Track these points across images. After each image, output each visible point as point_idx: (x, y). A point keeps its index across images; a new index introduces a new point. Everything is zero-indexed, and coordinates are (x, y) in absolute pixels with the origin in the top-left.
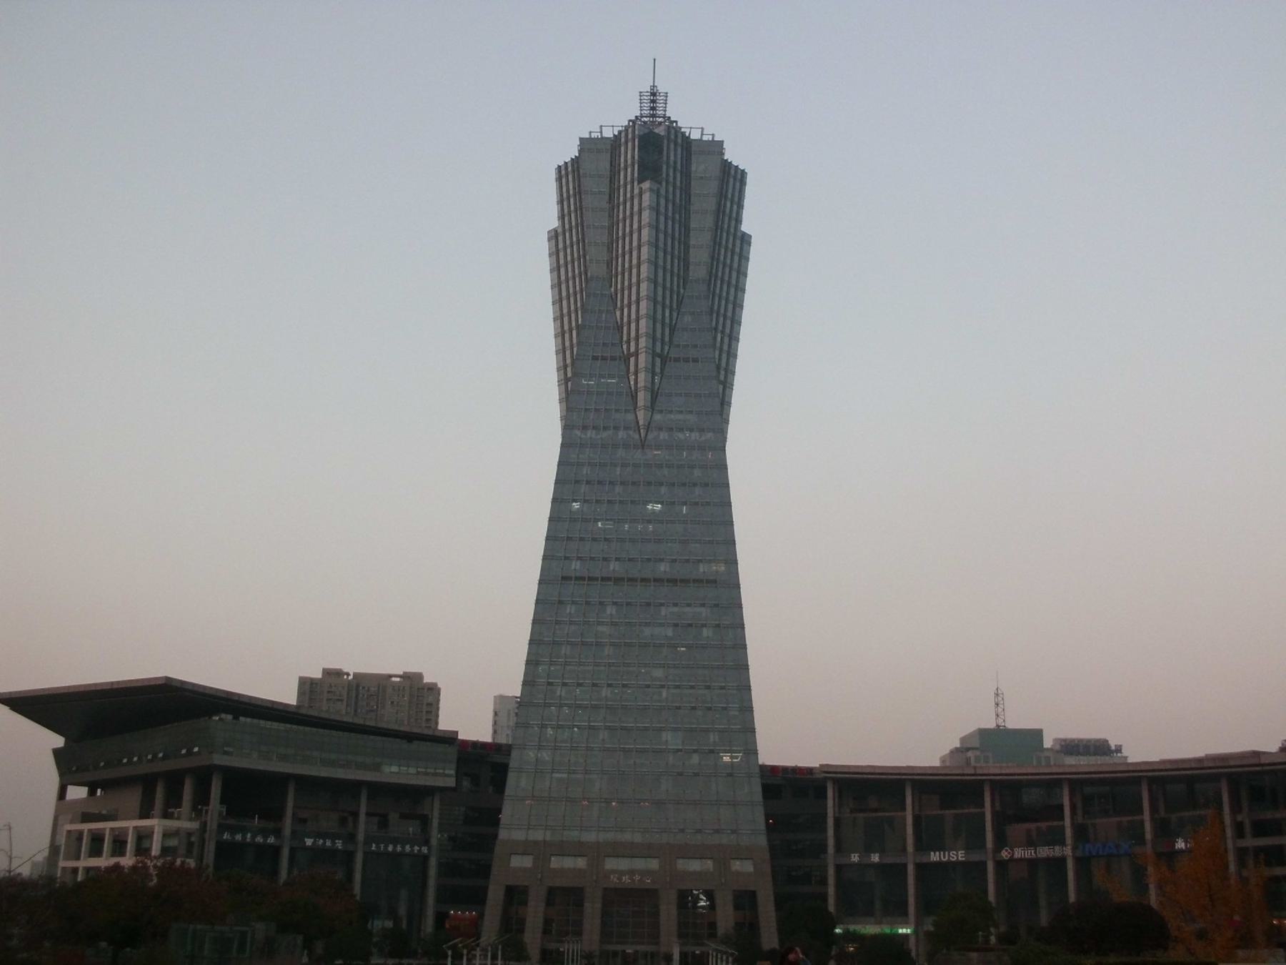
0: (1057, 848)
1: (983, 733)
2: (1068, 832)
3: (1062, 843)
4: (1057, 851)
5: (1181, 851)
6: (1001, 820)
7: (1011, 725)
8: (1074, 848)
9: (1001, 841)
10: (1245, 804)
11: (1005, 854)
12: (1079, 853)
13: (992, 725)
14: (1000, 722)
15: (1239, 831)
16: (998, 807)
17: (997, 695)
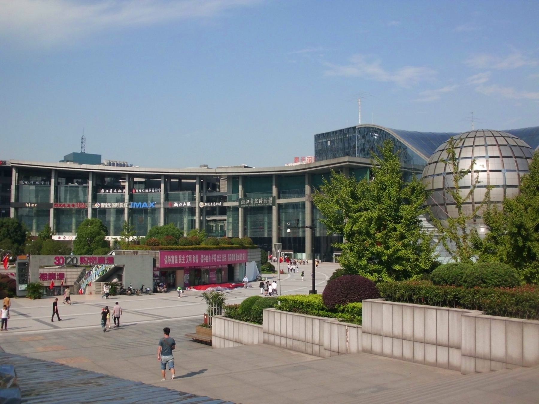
0: (121, 204)
1: (74, 154)
2: (127, 197)
3: (123, 201)
4: (121, 205)
5: (176, 207)
6: (96, 190)
7: (87, 152)
8: (128, 205)
9: (95, 199)
10: (204, 189)
11: (97, 206)
12: (131, 207)
13: (80, 152)
14: (83, 150)
15: (201, 200)
16: (94, 185)
17: (83, 138)
